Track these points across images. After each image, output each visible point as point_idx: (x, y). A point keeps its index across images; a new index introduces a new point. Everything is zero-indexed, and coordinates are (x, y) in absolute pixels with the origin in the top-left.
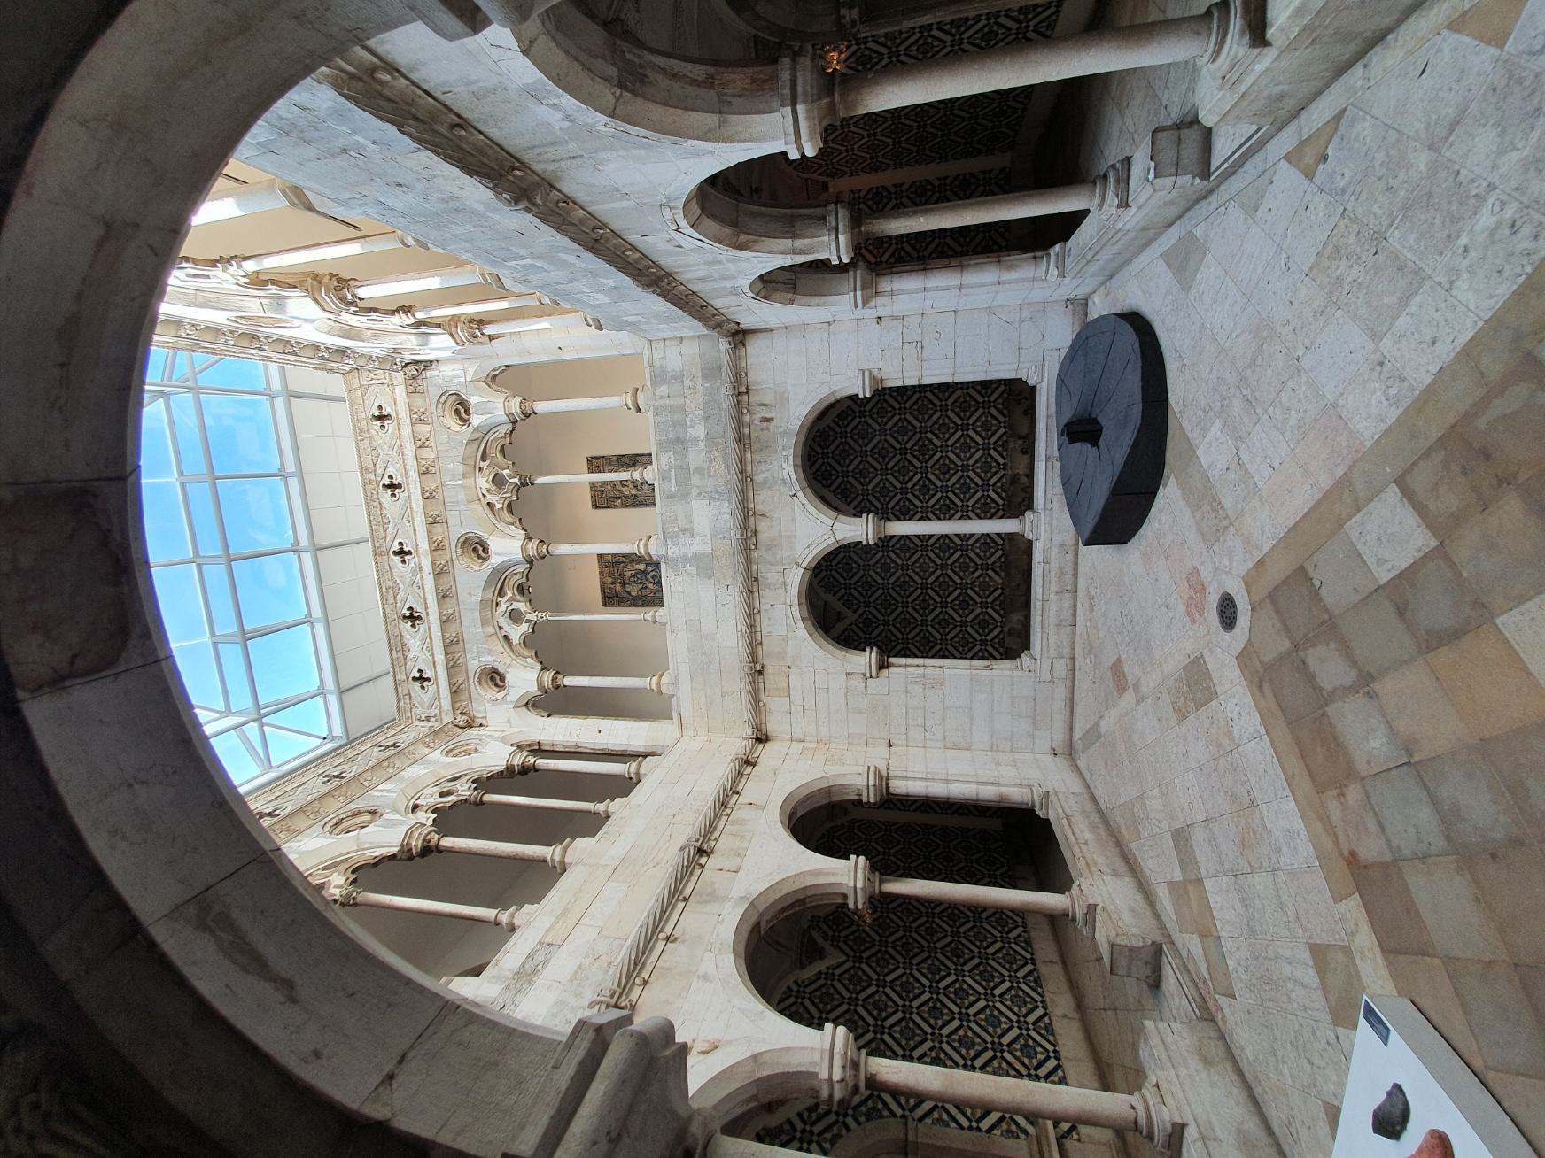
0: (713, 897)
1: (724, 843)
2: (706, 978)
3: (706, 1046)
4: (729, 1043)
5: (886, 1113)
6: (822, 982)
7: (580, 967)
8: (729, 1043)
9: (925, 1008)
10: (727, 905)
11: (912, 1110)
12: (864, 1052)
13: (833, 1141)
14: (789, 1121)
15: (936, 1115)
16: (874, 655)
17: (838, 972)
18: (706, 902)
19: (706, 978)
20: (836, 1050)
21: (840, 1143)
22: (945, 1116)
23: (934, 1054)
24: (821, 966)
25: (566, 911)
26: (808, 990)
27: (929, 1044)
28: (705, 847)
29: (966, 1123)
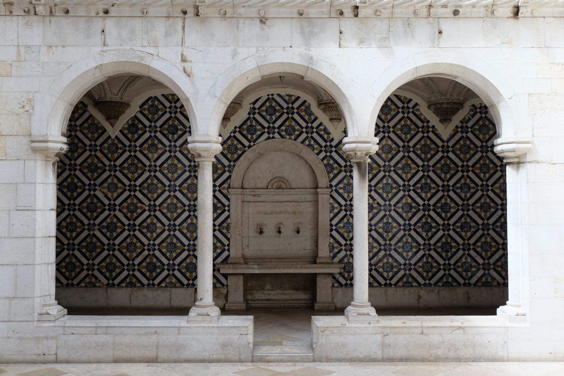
3: (188, 70)
4: (193, 83)
5: (332, 175)
8: (193, 83)
9: (409, 201)
10: (303, 50)
11: (337, 191)
12: (214, 160)
13: (309, 145)
14: (316, 118)
15: (336, 205)
16: (60, 146)
17: (431, 135)
18: (302, 32)
19: (235, 54)
20: (195, 144)
22: (336, 211)
23: (375, 205)
24: (434, 120)
26: (411, 116)
27: (382, 202)
29: (334, 222)
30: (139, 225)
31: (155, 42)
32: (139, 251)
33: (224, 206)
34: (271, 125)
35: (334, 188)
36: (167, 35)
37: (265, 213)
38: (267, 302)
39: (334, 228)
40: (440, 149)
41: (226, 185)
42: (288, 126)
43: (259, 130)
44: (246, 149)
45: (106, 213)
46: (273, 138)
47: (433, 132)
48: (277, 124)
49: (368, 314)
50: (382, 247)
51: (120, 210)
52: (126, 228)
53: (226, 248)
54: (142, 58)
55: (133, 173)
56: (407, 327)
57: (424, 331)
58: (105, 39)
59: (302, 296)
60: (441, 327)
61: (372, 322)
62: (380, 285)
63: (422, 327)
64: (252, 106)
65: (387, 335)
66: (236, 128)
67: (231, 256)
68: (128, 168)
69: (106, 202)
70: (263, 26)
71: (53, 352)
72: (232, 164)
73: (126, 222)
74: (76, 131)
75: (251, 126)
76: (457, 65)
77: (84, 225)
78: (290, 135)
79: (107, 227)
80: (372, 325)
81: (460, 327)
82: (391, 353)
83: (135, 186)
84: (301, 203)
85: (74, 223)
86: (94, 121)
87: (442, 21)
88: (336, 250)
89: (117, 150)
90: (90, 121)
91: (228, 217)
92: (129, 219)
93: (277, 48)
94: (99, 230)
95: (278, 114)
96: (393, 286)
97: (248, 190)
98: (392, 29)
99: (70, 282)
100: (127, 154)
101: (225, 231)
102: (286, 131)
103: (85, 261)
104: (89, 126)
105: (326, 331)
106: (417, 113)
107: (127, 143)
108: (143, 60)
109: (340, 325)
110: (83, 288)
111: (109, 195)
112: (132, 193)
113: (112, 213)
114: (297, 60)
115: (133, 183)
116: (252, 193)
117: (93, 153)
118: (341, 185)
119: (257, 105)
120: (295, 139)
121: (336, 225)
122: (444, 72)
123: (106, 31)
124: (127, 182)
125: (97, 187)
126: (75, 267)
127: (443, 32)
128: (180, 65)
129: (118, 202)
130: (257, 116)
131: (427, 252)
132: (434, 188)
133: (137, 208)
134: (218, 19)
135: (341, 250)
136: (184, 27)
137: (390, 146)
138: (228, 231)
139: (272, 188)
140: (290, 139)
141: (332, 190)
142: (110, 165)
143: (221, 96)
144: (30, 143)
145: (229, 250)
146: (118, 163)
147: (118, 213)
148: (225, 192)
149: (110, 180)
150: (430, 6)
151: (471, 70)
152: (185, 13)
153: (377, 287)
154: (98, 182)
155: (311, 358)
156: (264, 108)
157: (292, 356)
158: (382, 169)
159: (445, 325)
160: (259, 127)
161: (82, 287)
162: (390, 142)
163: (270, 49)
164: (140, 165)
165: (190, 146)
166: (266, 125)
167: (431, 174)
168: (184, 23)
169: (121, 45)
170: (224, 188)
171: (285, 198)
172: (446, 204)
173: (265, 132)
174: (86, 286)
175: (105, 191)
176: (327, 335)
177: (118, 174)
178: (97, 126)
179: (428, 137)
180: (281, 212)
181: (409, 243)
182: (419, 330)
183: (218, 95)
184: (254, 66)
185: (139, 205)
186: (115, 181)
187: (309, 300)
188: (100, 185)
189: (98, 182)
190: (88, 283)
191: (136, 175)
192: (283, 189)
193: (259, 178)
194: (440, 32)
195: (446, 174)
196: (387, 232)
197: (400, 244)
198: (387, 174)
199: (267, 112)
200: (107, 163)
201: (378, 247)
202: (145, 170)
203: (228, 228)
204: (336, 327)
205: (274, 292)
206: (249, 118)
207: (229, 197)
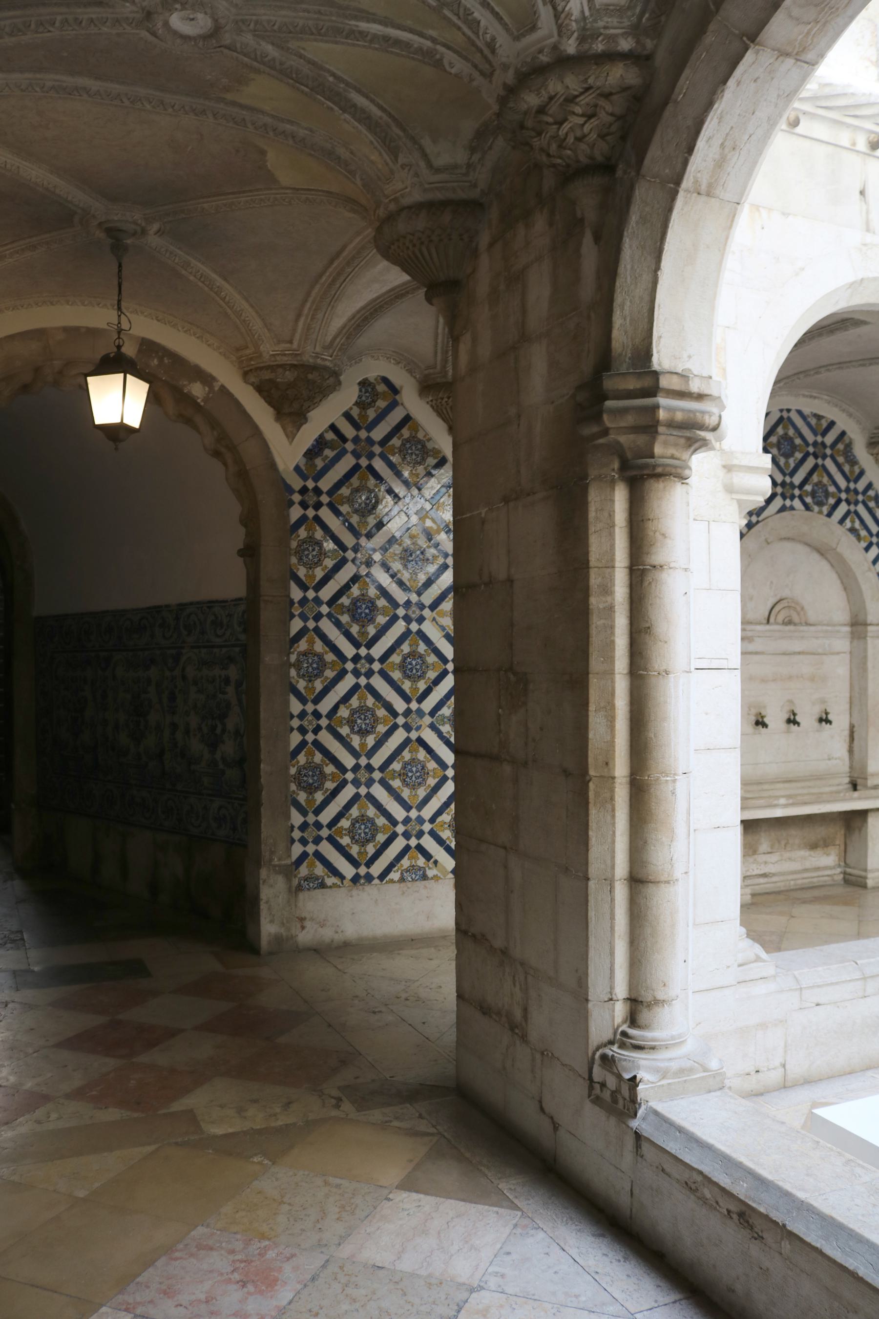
13: (852, 530)
21: (852, 538)
37: (764, 680)
38: (762, 880)
46: (792, 508)
58: (868, 212)
59: (827, 861)
71: (777, 1062)
74: (371, 456)
77: (395, 714)
84: (824, 657)
85: (368, 709)
86: (417, 431)
90: (406, 432)
99: (363, 870)
102: (813, 494)
103: (399, 813)
104: (403, 445)
110: (397, 885)
120: (829, 515)
123: (869, 192)
125: (427, 613)
126: (375, 830)
139: (776, 623)
140: (820, 512)
144: (721, 473)
171: (797, 646)
174: (402, 880)
178: (424, 446)
180: (790, 678)
187: (833, 868)
190: (407, 871)
192: (795, 624)
205: (774, 858)
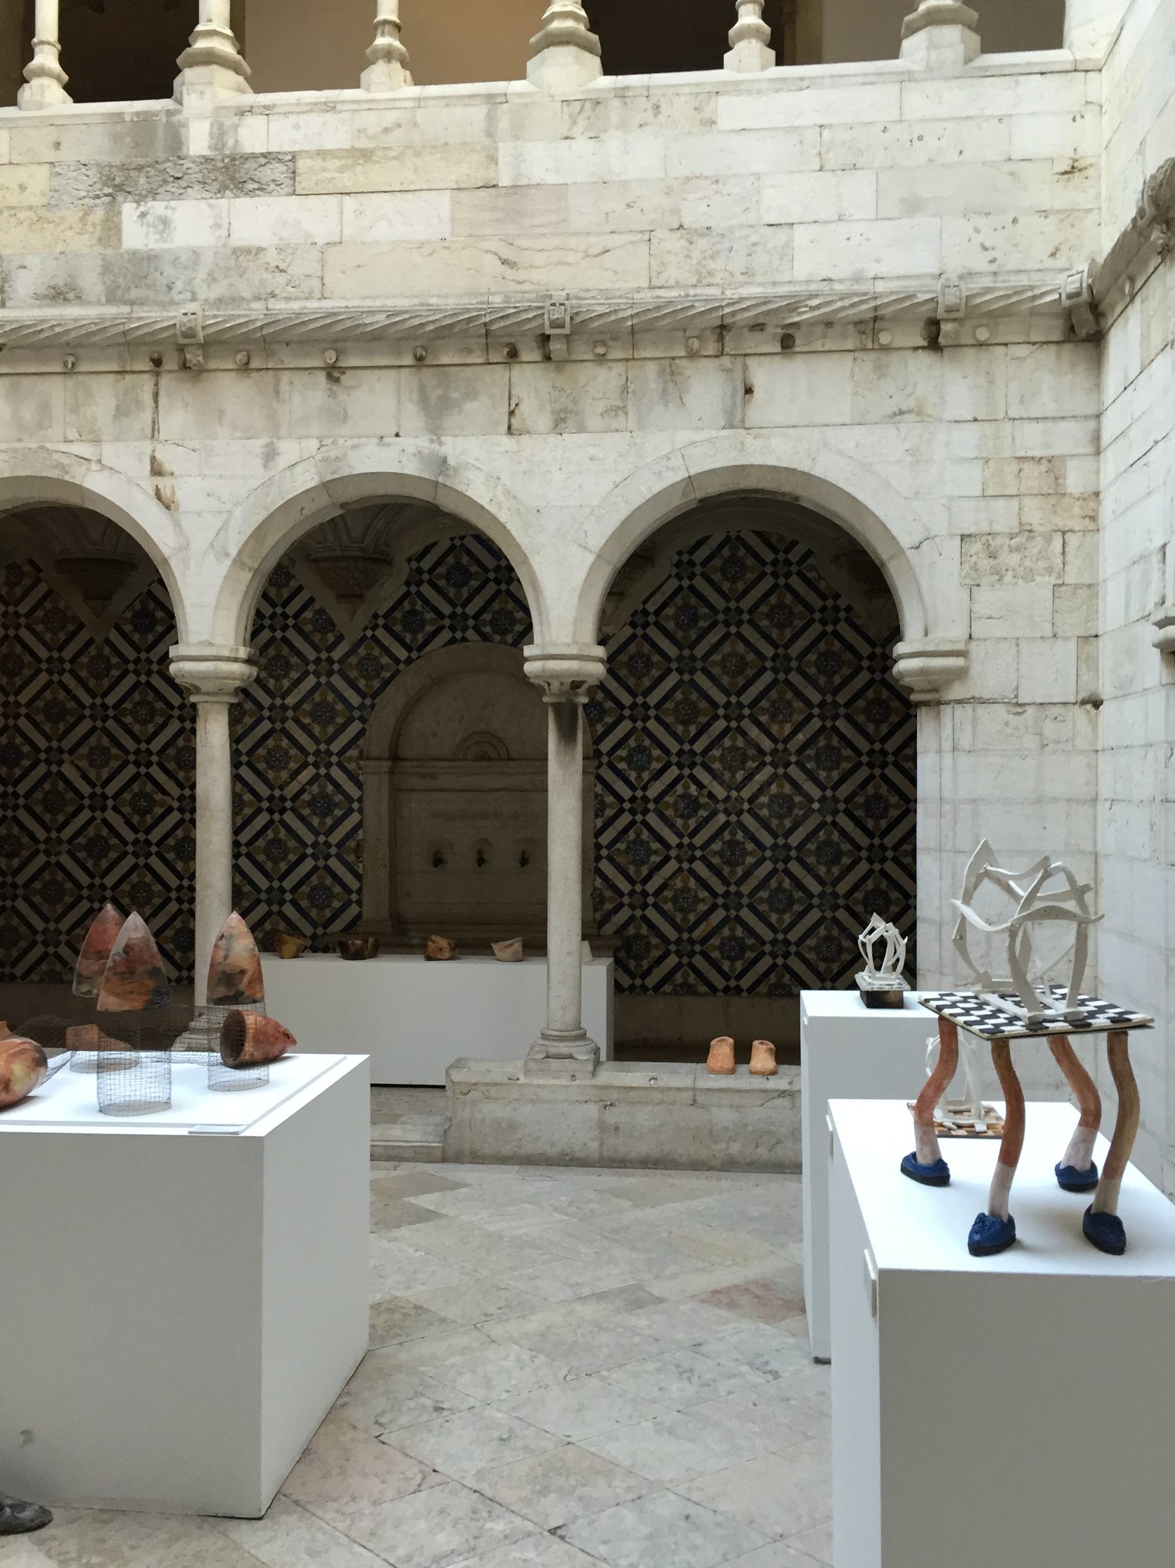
0: (436, 413)
1: (599, 382)
2: (270, 455)
3: (166, 493)
4: (177, 523)
5: (600, 728)
6: (817, 603)
7: (260, 250)
8: (177, 523)
10: (424, 443)
15: (609, 799)
17: (844, 629)
19: (270, 455)
22: (609, 812)
25: (366, 155)
28: (555, 347)
30: (158, 844)
31: (94, 431)
32: (157, 901)
33: (350, 799)
34: (459, 610)
35: (605, 759)
36: (120, 413)
39: (604, 852)
40: (865, 663)
41: (353, 752)
42: (498, 612)
43: (430, 622)
44: (402, 666)
45: (85, 815)
46: (464, 639)
47: (849, 621)
48: (471, 609)
49: (571, 1057)
50: (720, 901)
51: (115, 809)
52: (130, 848)
53: (354, 897)
54: (64, 468)
55: (144, 723)
56: (658, 1089)
57: (700, 1099)
60: (739, 1091)
61: (578, 1075)
62: (713, 989)
63: (694, 1089)
64: (414, 565)
65: (611, 1105)
66: (376, 616)
67: (364, 917)
68: (133, 713)
69: (86, 790)
70: (335, 388)
72: (368, 701)
73: (130, 836)
75: (413, 612)
76: (786, 469)
78: (504, 633)
79: (88, 848)
80: (577, 1082)
81: (784, 1092)
82: (620, 1145)
83: (149, 753)
87: (752, 362)
88: (608, 906)
89: (108, 671)
91: (359, 825)
92: (135, 830)
93: (364, 440)
94: (69, 852)
95: (475, 584)
96: (745, 994)
97: (408, 764)
98: (632, 387)
100: (131, 680)
101: (351, 858)
102: (493, 623)
103: (39, 925)
105: (472, 1094)
106: (809, 575)
107: (131, 654)
108: (67, 472)
109: (505, 1080)
111: (92, 773)
112: (143, 770)
113: (98, 814)
114: (411, 468)
115: (143, 746)
116: (419, 770)
117: (56, 678)
118: (622, 753)
119: (426, 564)
121: (609, 847)
122: (762, 485)
124: (131, 745)
125: (65, 756)
127: (756, 390)
128: (148, 484)
129: (111, 790)
130: (426, 589)
131: (829, 914)
132: (848, 759)
133: (153, 803)
134: (233, 374)
135: (621, 905)
136: (156, 395)
137: (743, 658)
138: (358, 857)
140: (503, 642)
141: (600, 765)
142: (93, 706)
143: (240, 553)
145: (359, 903)
146: (111, 700)
147: (110, 815)
148: (351, 766)
149: (93, 740)
150: (722, 327)
151: (824, 481)
152: (157, 362)
153: (704, 994)
154: (67, 743)
155: (439, 1153)
156: (442, 570)
157: (394, 1147)
158: (721, 712)
159: (749, 1087)
160: (429, 616)
161: (32, 981)
162: (741, 648)
163: (349, 443)
164: (159, 705)
165: (173, 668)
166: (446, 609)
167: (841, 724)
168: (156, 385)
169: (20, 440)
170: (350, 759)
172: (878, 797)
173: (443, 627)
174: (41, 981)
175: (84, 764)
176: (474, 1102)
177: (111, 724)
179: (836, 634)
181: (785, 890)
182: (687, 1097)
183: (234, 551)
184: (313, 484)
185: (159, 797)
186: (106, 741)
188: (72, 751)
189: (67, 743)
191: (151, 728)
192: (490, 759)
193: (435, 735)
194: (749, 391)
195: (878, 723)
196: (732, 864)
197: (764, 894)
198: (734, 724)
199: (448, 580)
200: (87, 700)
201: (710, 901)
202: (171, 716)
203: (358, 851)
204: (496, 1084)
206: (407, 594)
207: (361, 778)
